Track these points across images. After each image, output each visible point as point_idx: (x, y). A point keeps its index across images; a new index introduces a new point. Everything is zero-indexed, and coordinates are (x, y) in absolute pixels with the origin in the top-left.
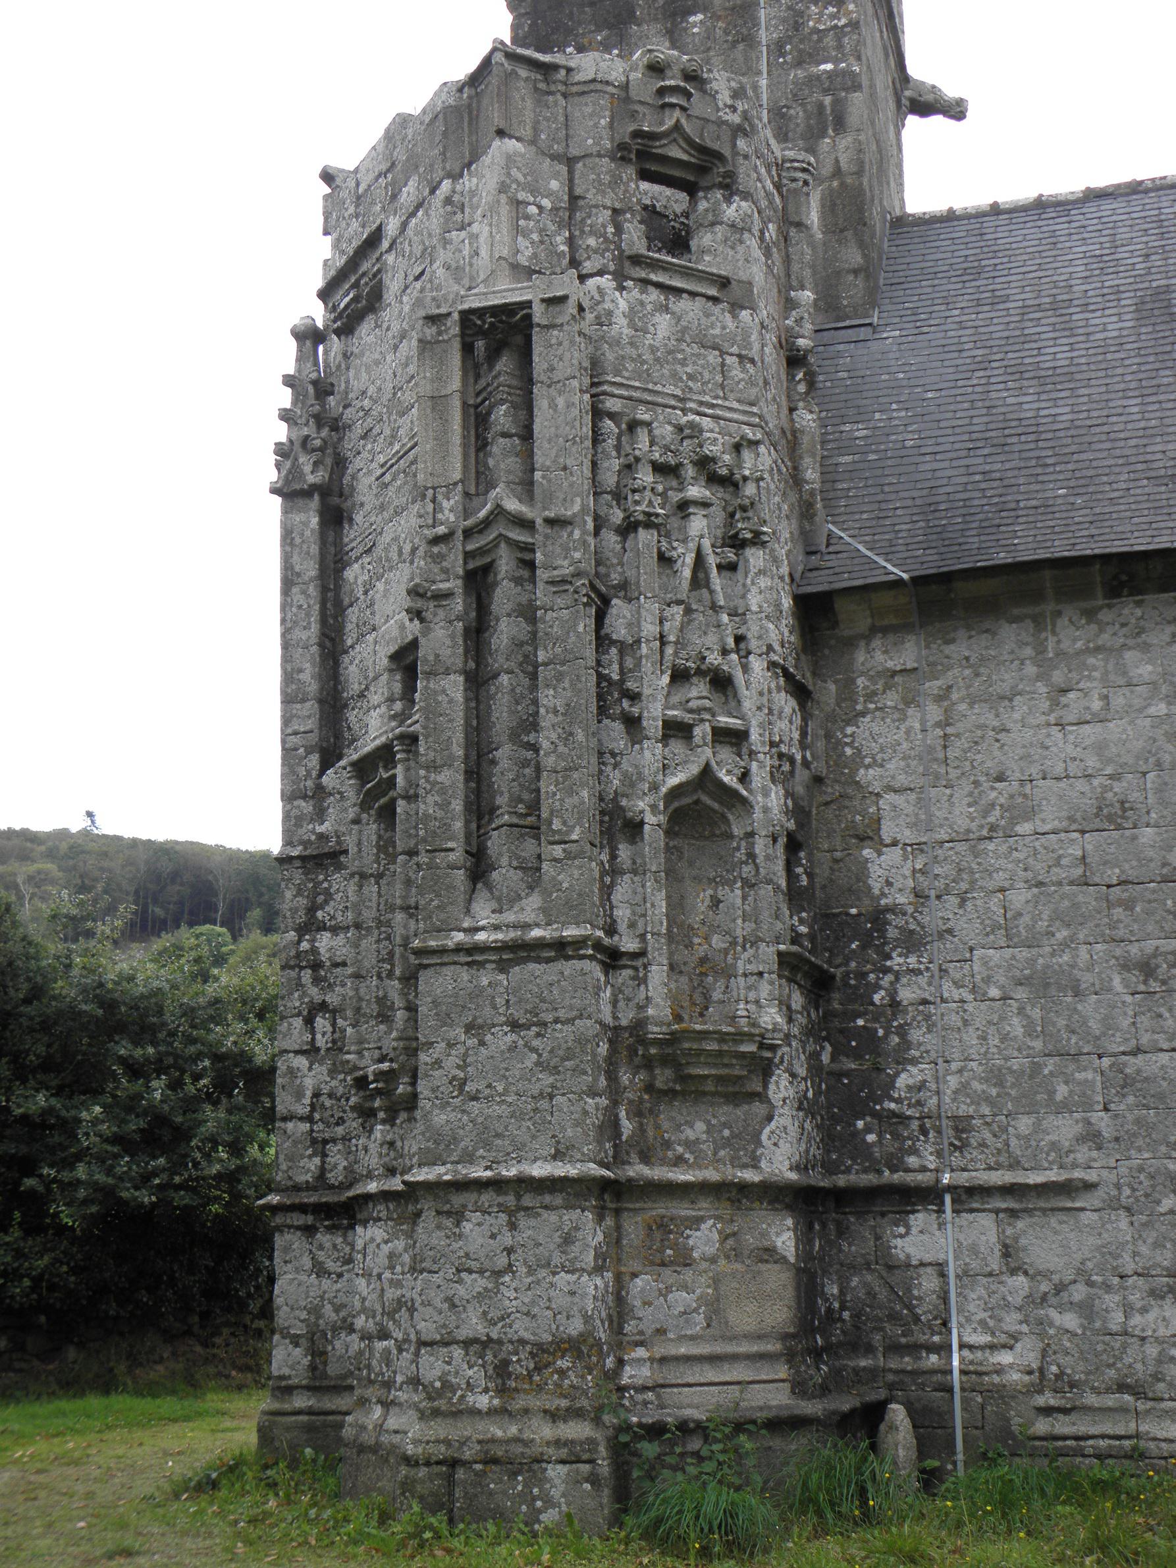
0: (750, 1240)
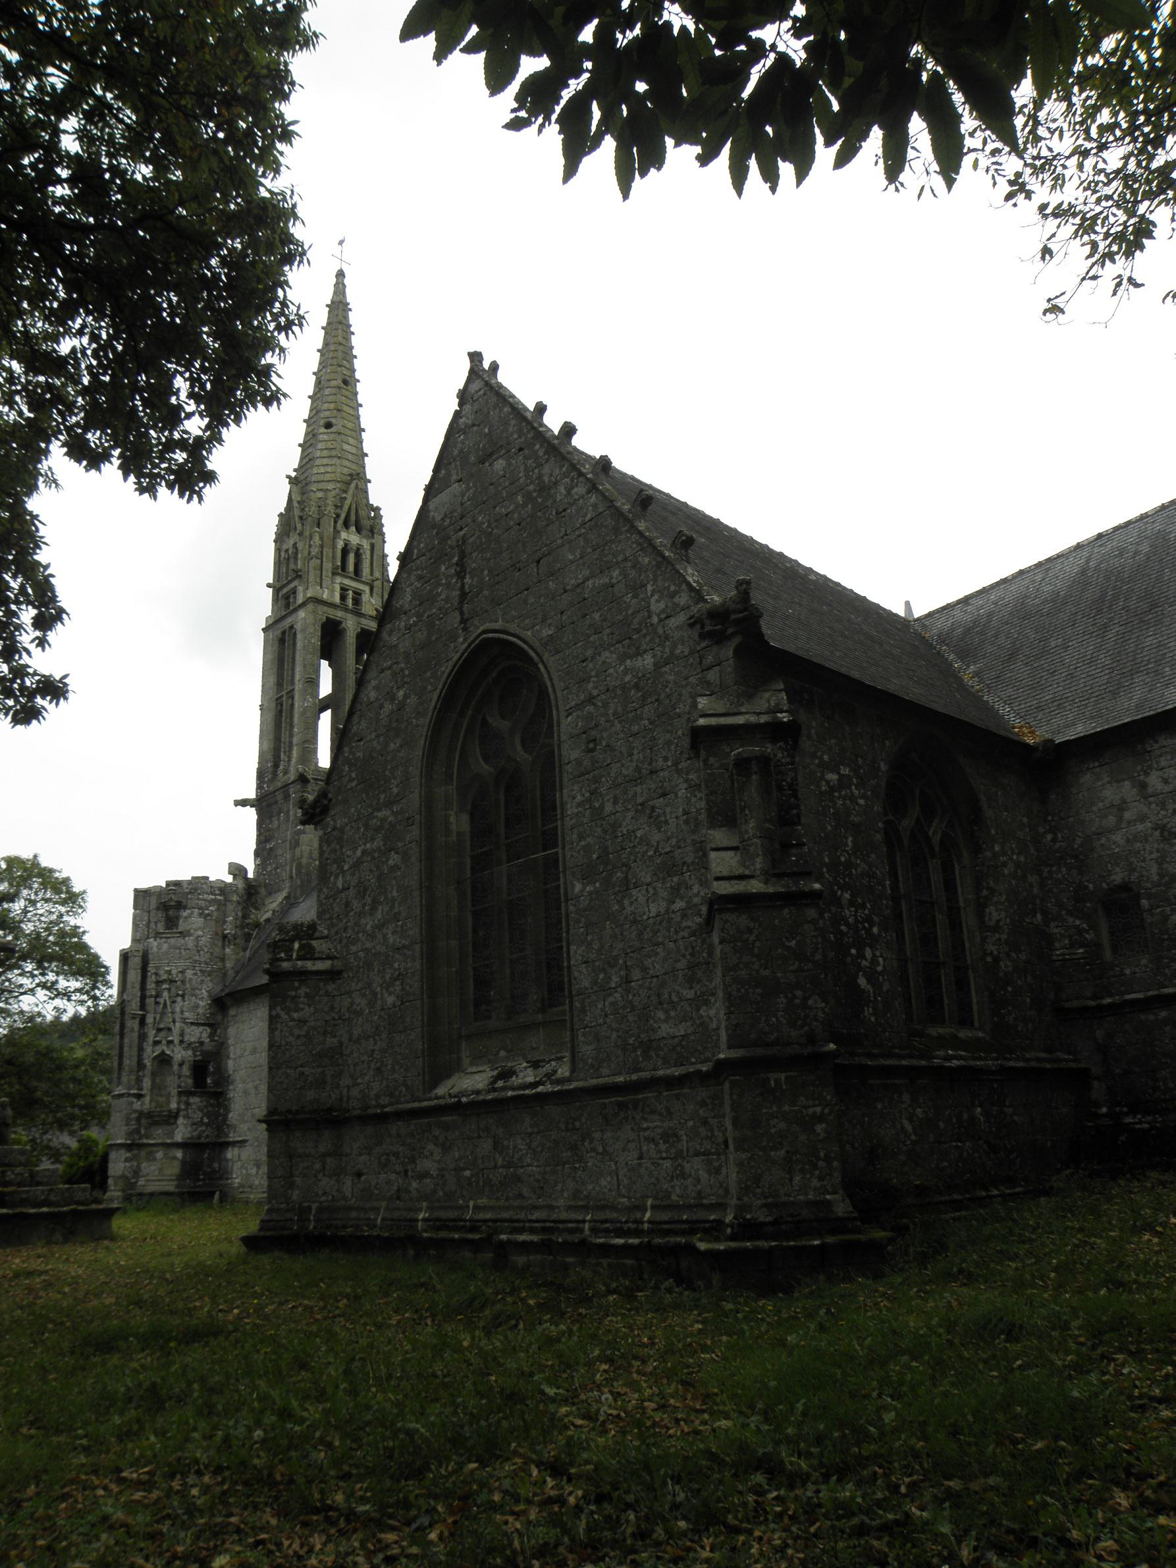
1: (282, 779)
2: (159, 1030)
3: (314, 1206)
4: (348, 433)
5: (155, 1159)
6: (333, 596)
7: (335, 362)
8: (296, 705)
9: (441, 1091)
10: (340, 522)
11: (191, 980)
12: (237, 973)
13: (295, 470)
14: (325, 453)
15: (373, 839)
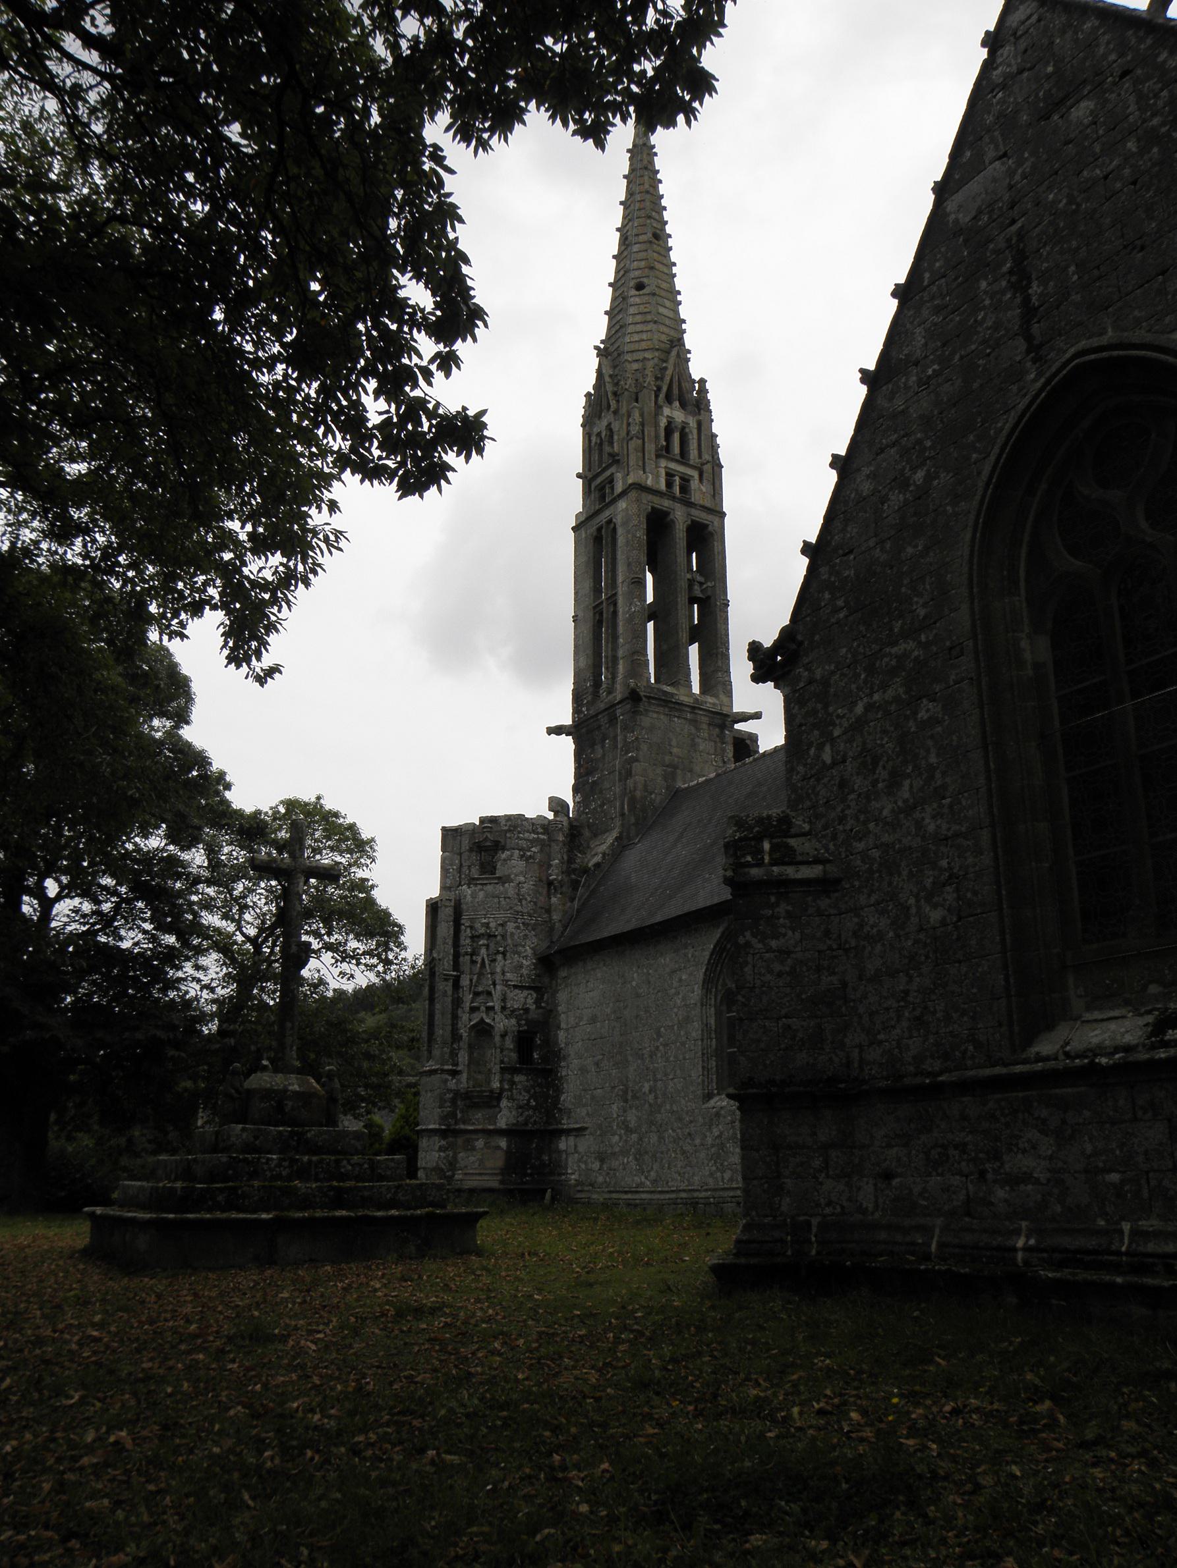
0: (493, 1144)
1: (605, 699)
2: (477, 994)
3: (815, 1221)
4: (663, 293)
5: (474, 1149)
6: (658, 483)
7: (642, 213)
8: (620, 611)
9: (1046, 1046)
10: (662, 396)
11: (512, 934)
12: (566, 927)
13: (602, 342)
14: (639, 318)
15: (884, 687)
